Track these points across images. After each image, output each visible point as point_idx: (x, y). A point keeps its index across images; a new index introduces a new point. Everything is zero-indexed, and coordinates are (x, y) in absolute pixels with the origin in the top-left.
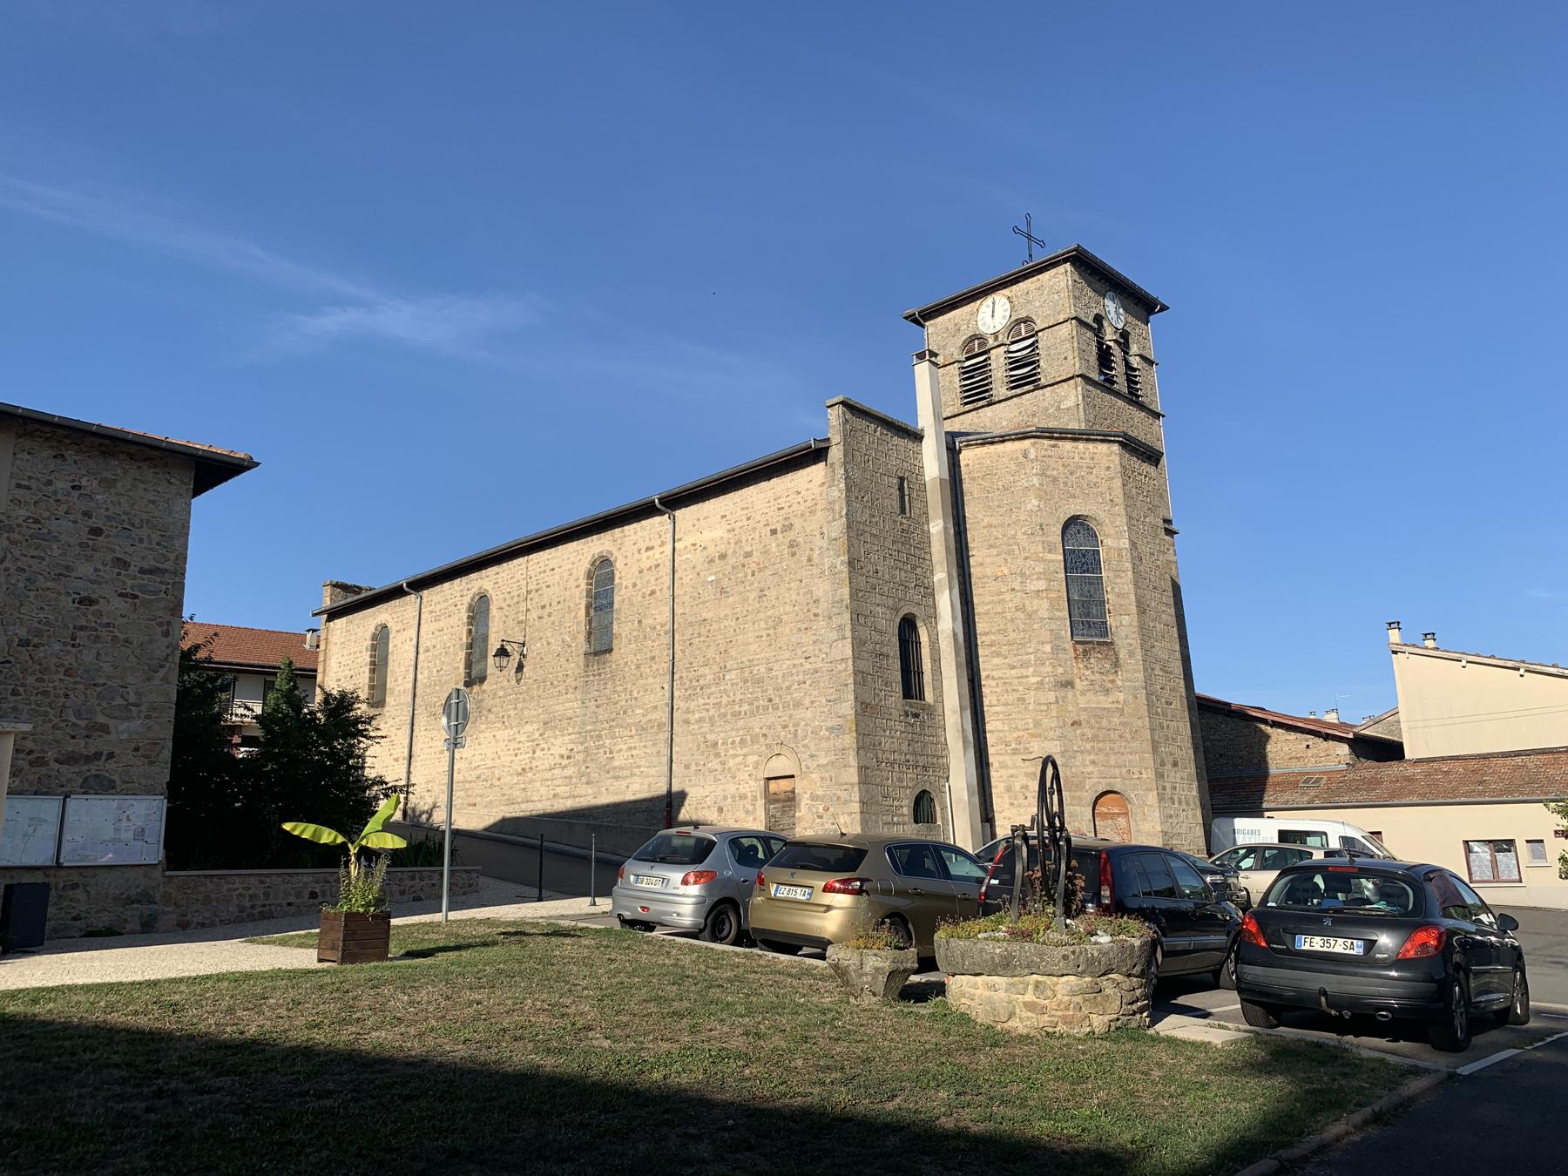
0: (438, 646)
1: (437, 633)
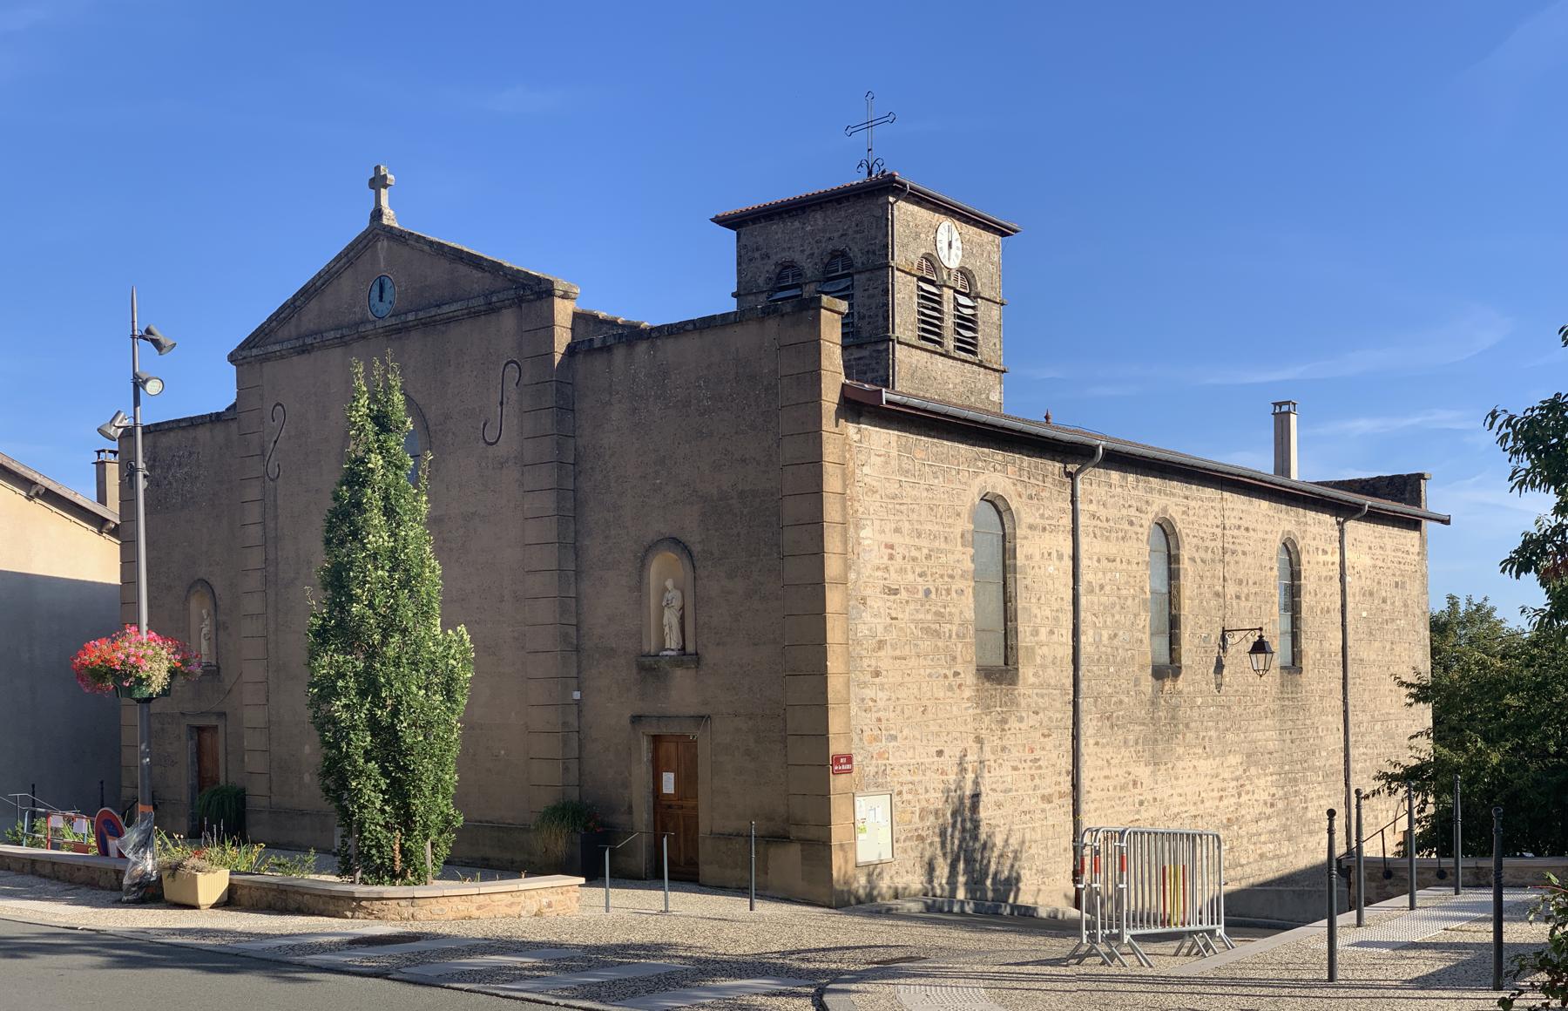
0: (1107, 588)
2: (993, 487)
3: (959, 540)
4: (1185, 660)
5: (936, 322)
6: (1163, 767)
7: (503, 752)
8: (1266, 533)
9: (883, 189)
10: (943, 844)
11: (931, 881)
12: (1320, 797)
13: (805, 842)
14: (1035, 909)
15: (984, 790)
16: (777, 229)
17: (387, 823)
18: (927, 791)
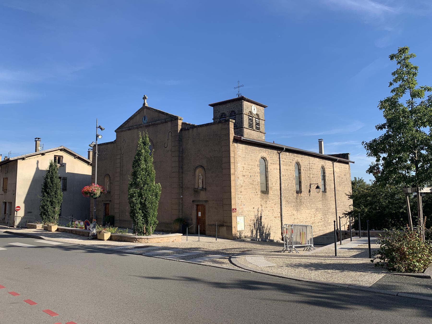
0: (286, 175)
2: (263, 156)
3: (257, 166)
4: (303, 190)
5: (252, 124)
6: (299, 212)
7: (167, 208)
8: (318, 165)
9: (241, 99)
10: (255, 227)
11: (252, 234)
12: (331, 218)
13: (227, 226)
14: (274, 240)
15: (263, 215)
16: (221, 107)
17: (143, 223)
18: (251, 216)
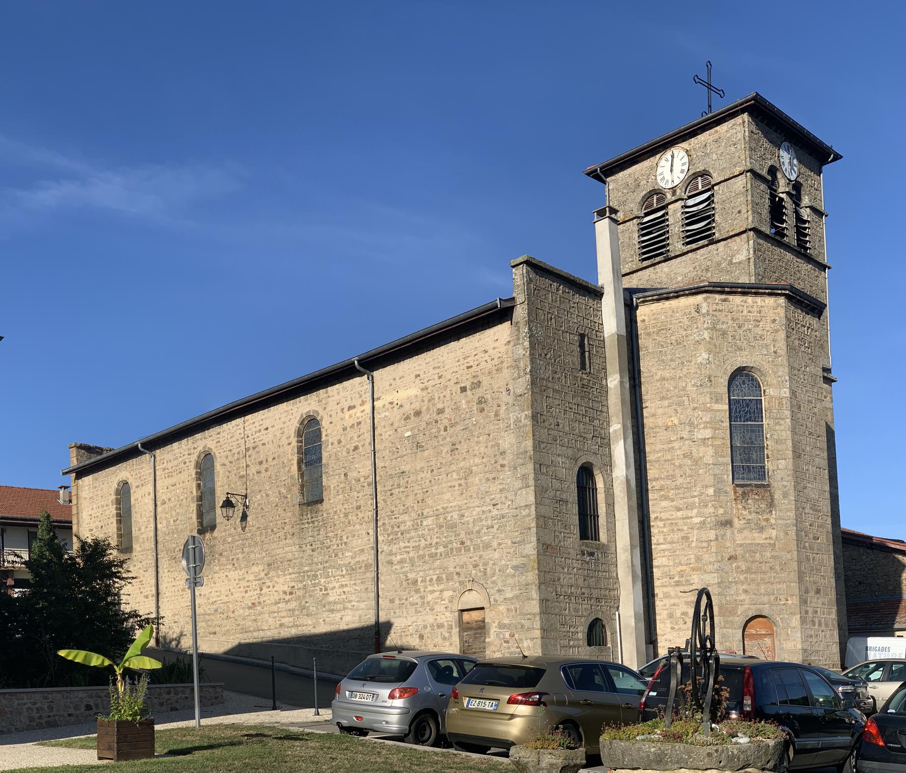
0: (173, 499)
1: (171, 488)
